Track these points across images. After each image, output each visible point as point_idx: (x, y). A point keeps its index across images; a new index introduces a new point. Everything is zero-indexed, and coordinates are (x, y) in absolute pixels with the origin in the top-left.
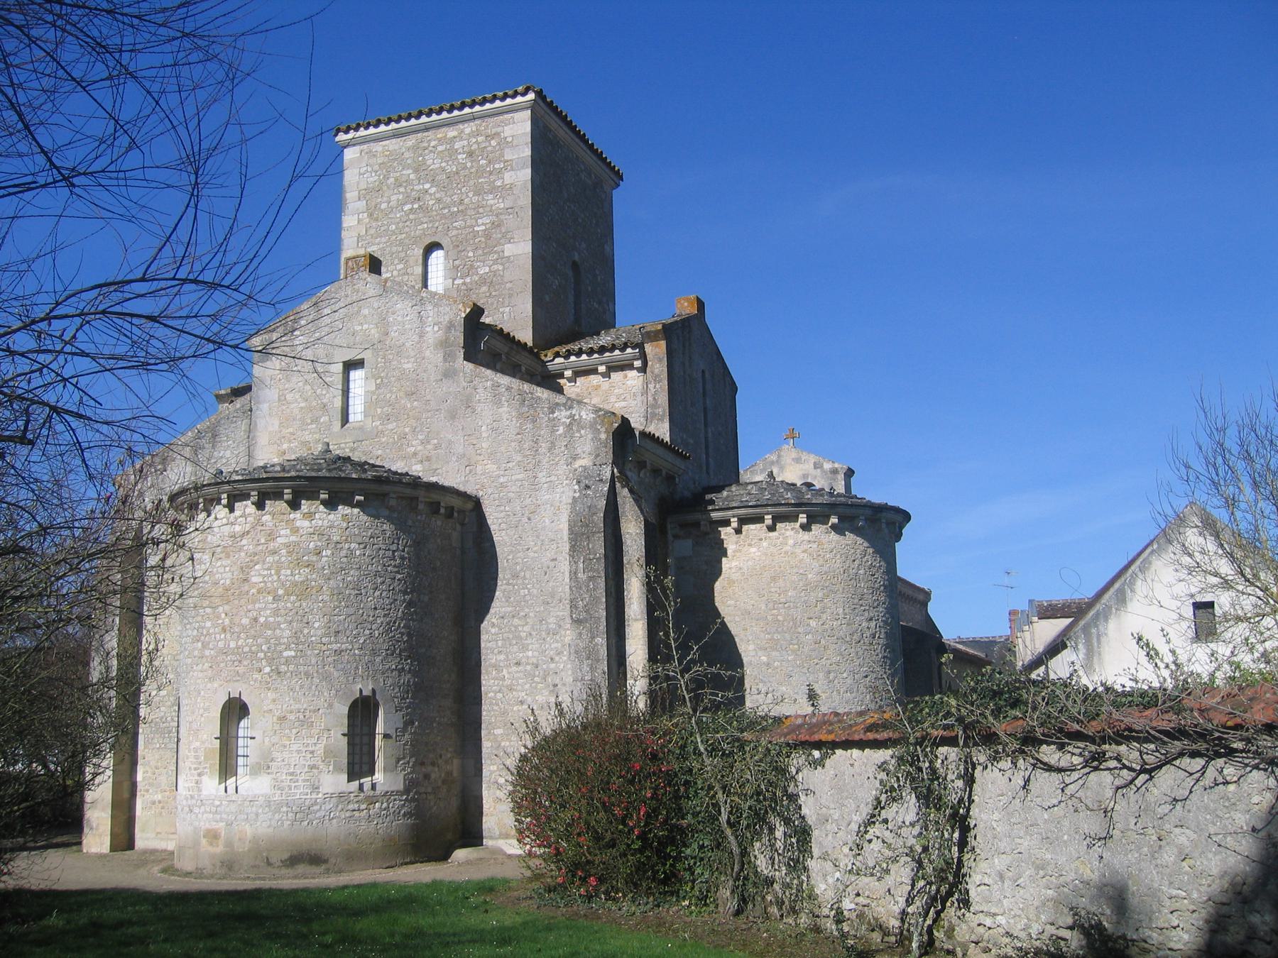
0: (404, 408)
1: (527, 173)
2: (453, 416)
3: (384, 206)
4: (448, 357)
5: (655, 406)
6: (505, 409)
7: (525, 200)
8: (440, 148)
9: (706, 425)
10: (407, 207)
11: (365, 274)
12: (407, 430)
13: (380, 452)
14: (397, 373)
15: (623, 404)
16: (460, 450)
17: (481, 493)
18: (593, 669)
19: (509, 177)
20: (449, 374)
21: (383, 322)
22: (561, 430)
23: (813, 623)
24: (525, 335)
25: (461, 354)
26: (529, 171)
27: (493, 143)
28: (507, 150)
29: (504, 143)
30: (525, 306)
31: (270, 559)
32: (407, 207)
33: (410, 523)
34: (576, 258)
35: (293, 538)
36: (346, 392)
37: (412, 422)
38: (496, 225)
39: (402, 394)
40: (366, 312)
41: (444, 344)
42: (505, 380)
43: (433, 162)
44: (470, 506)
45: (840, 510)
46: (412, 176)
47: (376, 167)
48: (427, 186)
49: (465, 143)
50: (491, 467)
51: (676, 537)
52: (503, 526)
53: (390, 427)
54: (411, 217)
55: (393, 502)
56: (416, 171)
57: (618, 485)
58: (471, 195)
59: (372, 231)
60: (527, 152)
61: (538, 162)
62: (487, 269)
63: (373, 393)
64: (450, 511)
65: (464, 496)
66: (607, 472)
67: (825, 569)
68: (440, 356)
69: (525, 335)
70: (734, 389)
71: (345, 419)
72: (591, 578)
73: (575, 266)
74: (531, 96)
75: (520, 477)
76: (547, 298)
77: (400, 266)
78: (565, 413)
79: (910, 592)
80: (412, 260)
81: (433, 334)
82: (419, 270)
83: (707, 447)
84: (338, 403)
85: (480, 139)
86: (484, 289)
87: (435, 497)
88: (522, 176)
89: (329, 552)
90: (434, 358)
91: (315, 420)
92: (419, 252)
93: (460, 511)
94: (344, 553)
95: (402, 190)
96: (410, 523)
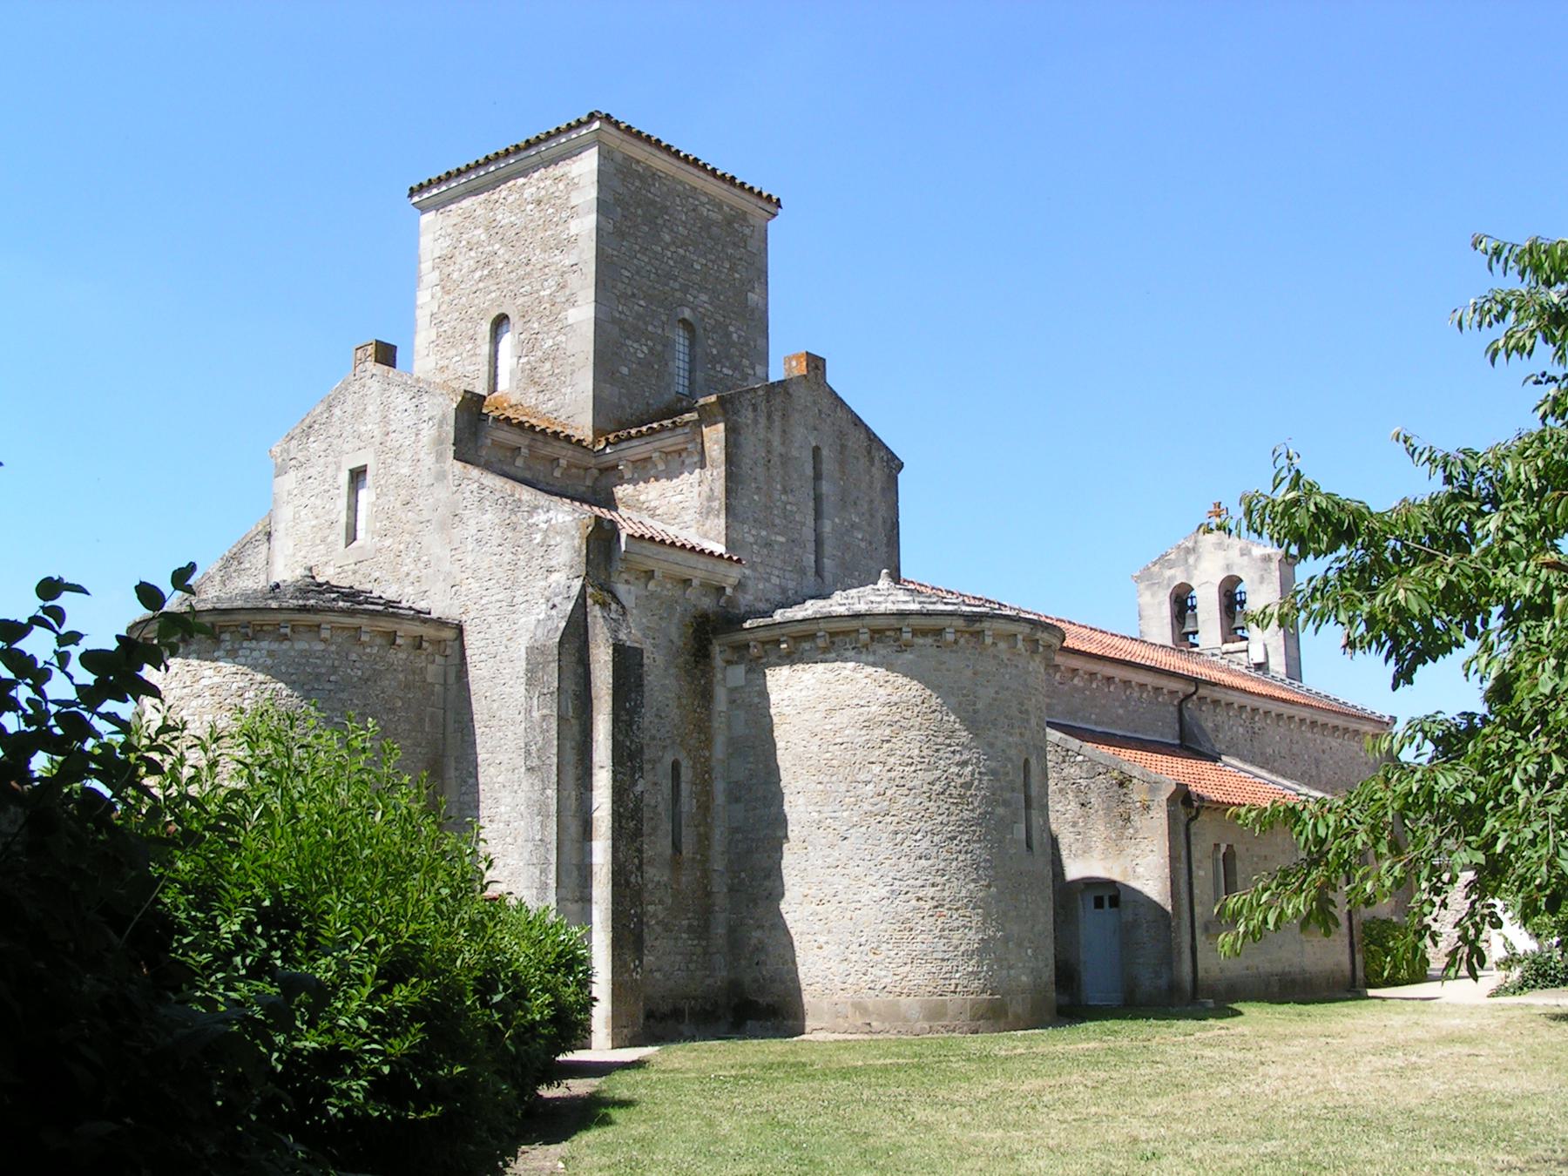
0: (400, 521)
1: (590, 220)
2: (443, 527)
3: (455, 276)
4: (440, 457)
5: (710, 499)
6: (489, 516)
7: (590, 255)
8: (510, 199)
9: (818, 515)
10: (477, 275)
11: (372, 367)
12: (402, 547)
13: (377, 574)
14: (394, 480)
15: (679, 498)
16: (446, 567)
17: (464, 618)
18: (543, 826)
19: (574, 227)
20: (441, 476)
21: (385, 419)
22: (538, 537)
23: (876, 769)
24: (582, 425)
25: (450, 451)
26: (593, 217)
27: (561, 186)
28: (573, 194)
29: (573, 185)
30: (585, 383)
31: (194, 703)
32: (477, 275)
33: (354, 657)
34: (687, 313)
35: (217, 680)
36: (353, 508)
37: (406, 537)
38: (562, 287)
39: (398, 504)
40: (370, 409)
41: (439, 441)
42: (491, 480)
43: (504, 217)
44: (449, 634)
45: (867, 621)
46: (483, 237)
47: (450, 230)
48: (497, 246)
49: (534, 189)
50: (475, 586)
51: (729, 662)
52: (484, 657)
53: (388, 542)
54: (481, 285)
55: (325, 634)
56: (487, 229)
57: (590, 601)
58: (538, 252)
59: (444, 307)
60: (593, 193)
61: (603, 207)
62: (550, 342)
63: (374, 504)
64: (418, 642)
65: (440, 623)
66: (577, 584)
67: (894, 699)
68: (432, 458)
69: (582, 425)
70: (894, 465)
71: (351, 536)
72: (544, 717)
73: (684, 321)
74: (597, 125)
75: (500, 597)
76: (625, 370)
77: (469, 347)
78: (543, 517)
79: (1340, 722)
80: (479, 337)
81: (428, 432)
82: (485, 349)
83: (819, 542)
84: (343, 519)
85: (548, 182)
86: (548, 365)
87: (386, 625)
88: (585, 225)
89: (252, 694)
90: (428, 460)
91: (323, 541)
92: (486, 327)
93: (431, 642)
94: (266, 695)
95: (472, 254)
96: (354, 657)
